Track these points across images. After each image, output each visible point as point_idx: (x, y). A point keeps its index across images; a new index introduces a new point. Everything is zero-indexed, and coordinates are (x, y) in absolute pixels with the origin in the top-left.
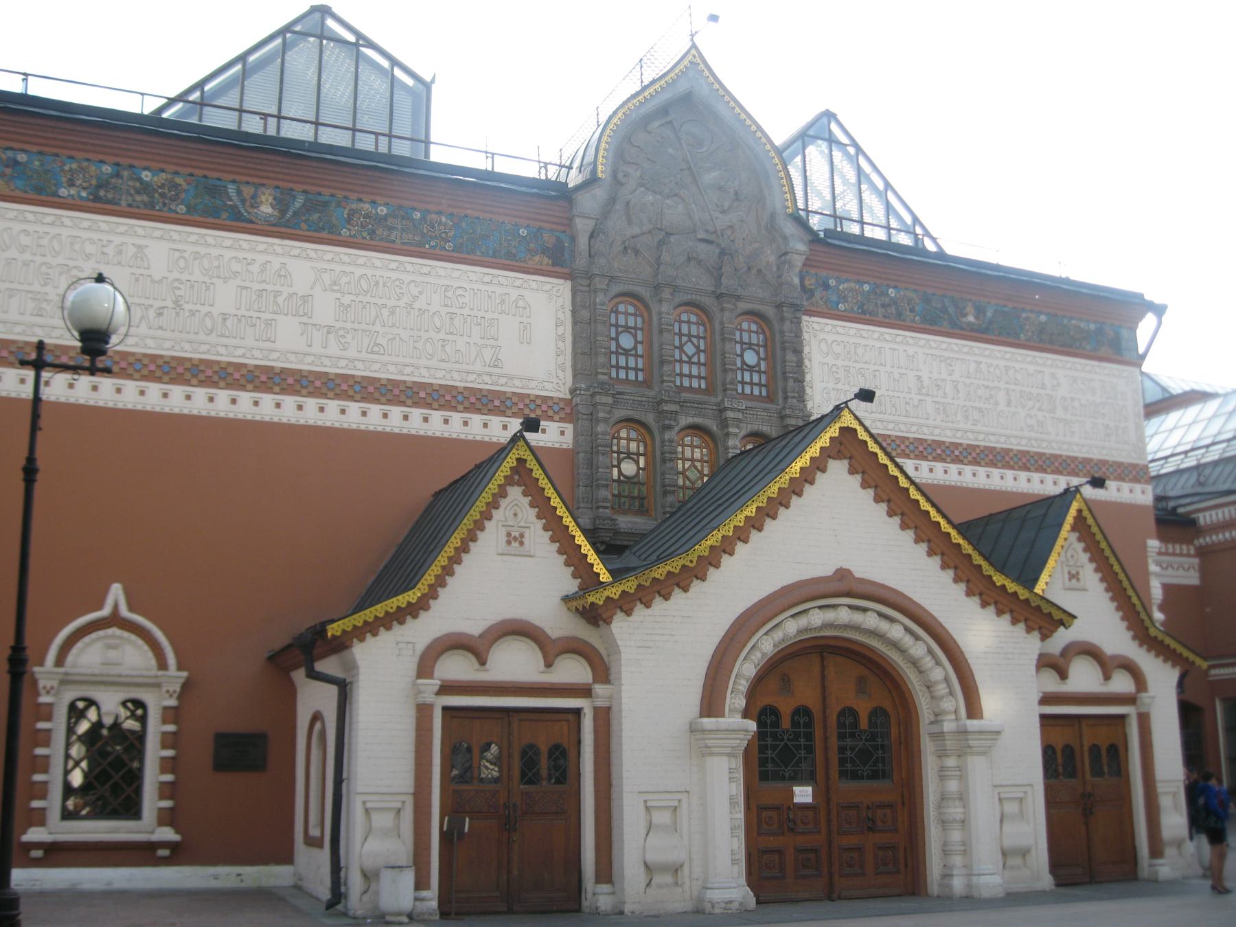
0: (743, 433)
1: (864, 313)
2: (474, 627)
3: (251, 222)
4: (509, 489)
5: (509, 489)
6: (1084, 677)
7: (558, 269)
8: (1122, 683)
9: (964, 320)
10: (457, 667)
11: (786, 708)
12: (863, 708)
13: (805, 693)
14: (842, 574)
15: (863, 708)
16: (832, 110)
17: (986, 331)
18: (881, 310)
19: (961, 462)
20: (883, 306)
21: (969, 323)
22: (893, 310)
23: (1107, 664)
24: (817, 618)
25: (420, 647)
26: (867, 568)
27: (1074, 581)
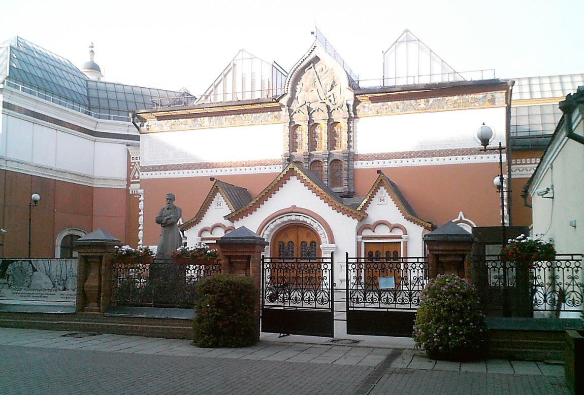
0: (330, 161)
1: (378, 113)
2: (210, 226)
3: (203, 126)
4: (217, 193)
5: (217, 193)
6: (383, 231)
7: (279, 121)
8: (397, 232)
9: (420, 106)
10: (207, 235)
11: (286, 241)
12: (308, 242)
13: (292, 237)
14: (294, 207)
15: (308, 242)
16: (409, 29)
17: (430, 108)
18: (385, 111)
19: (414, 157)
20: (386, 109)
21: (421, 108)
22: (390, 109)
23: (394, 227)
24: (286, 219)
25: (199, 230)
26: (300, 205)
27: (382, 202)
